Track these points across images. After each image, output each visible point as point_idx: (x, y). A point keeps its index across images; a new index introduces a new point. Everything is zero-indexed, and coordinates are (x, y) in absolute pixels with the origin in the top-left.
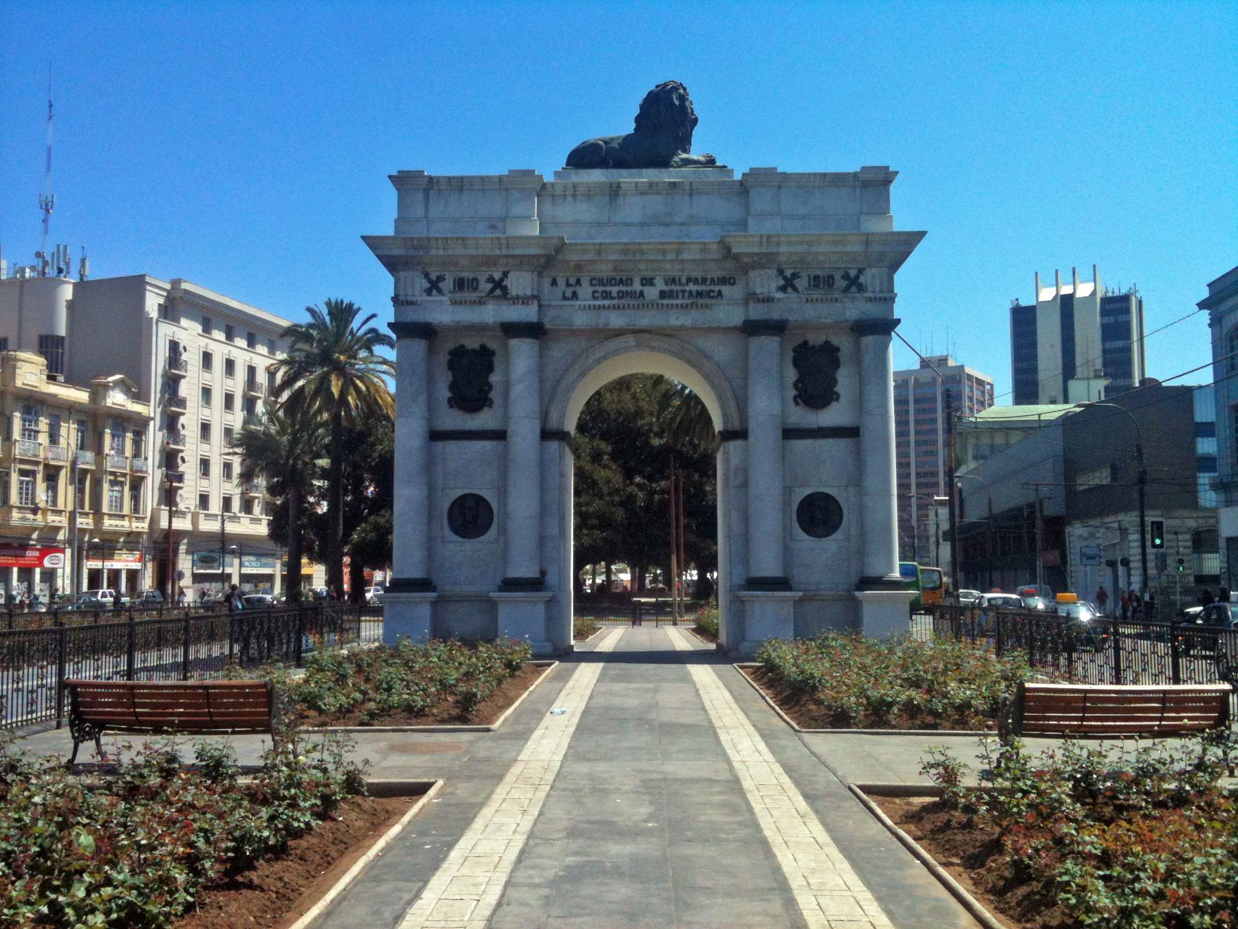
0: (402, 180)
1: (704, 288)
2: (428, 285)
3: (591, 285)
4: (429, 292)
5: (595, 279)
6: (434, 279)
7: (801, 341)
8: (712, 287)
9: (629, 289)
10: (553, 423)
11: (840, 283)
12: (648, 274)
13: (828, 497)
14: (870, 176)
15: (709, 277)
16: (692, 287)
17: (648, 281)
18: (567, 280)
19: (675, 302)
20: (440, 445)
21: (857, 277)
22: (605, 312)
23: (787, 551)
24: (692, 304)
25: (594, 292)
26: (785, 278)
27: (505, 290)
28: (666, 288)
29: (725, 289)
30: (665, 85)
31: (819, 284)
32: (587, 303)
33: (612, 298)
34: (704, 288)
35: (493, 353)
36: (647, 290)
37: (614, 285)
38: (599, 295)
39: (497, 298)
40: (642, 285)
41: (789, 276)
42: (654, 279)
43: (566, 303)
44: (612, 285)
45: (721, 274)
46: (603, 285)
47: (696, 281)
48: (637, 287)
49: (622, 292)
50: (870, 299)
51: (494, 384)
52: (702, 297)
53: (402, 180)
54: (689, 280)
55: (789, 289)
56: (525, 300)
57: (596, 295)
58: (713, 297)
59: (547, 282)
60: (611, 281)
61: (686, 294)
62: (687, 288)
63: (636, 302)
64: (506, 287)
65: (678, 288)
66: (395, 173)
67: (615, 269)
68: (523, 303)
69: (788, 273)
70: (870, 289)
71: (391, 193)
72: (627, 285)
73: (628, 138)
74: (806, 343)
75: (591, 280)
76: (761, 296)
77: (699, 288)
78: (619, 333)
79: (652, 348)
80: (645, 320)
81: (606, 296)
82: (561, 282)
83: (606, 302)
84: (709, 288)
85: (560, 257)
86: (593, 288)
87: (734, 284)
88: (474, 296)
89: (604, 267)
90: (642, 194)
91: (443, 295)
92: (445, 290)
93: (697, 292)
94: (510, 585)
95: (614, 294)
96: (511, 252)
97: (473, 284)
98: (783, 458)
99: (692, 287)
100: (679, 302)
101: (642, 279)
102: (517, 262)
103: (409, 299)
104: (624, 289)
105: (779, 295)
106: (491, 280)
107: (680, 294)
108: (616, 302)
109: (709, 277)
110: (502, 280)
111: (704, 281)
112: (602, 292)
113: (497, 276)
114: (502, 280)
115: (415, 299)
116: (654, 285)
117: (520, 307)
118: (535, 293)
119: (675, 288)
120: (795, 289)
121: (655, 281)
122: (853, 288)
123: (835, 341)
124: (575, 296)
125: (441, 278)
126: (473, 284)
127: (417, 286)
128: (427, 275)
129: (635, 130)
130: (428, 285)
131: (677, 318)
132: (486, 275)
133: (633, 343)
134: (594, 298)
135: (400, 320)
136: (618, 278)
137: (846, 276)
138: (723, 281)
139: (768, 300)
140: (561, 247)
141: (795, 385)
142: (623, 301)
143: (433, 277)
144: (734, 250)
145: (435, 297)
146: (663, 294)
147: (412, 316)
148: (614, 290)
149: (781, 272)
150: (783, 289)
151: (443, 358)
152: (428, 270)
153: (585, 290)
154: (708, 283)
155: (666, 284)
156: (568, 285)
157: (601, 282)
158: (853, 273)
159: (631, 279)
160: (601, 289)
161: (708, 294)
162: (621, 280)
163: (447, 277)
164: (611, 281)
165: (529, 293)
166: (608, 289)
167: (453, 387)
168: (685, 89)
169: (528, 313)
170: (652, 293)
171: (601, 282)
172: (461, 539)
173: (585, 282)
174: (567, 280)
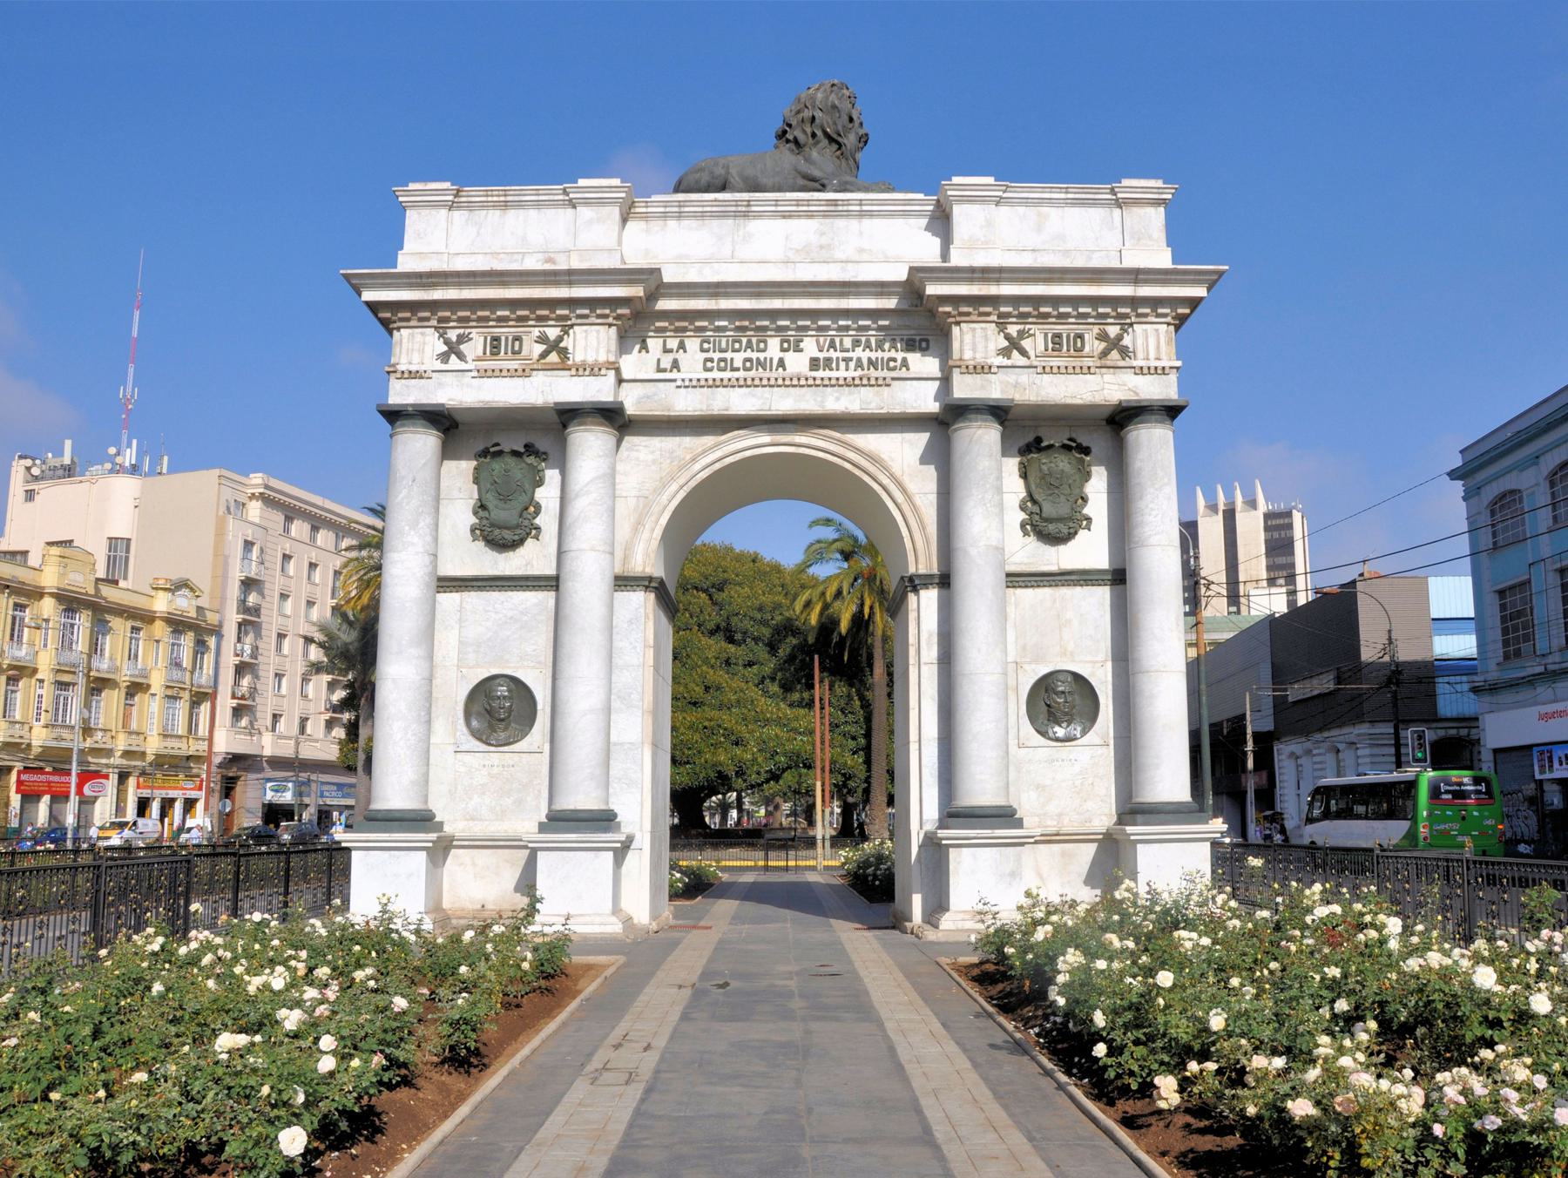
1: (879, 354)
2: (445, 348)
8: (893, 354)
9: (762, 356)
19: (834, 374)
27: (563, 353)
28: (821, 355)
33: (734, 369)
36: (790, 357)
37: (738, 351)
38: (715, 364)
40: (783, 350)
41: (1015, 335)
44: (734, 351)
46: (721, 351)
47: (868, 346)
51: (543, 503)
54: (856, 343)
55: (1015, 353)
56: (594, 370)
57: (709, 365)
58: (894, 369)
61: (852, 365)
64: (566, 349)
65: (841, 355)
68: (592, 374)
70: (1140, 354)
76: (972, 363)
77: (873, 355)
81: (725, 365)
83: (727, 375)
84: (887, 355)
93: (869, 359)
95: (736, 365)
100: (842, 373)
103: (413, 368)
104: (754, 355)
105: (1001, 361)
106: (542, 339)
107: (842, 365)
108: (741, 374)
110: (560, 339)
112: (721, 360)
114: (560, 339)
115: (422, 368)
116: (801, 351)
118: (612, 359)
119: (833, 354)
122: (1115, 354)
127: (428, 349)
130: (445, 348)
131: (838, 399)
132: (536, 332)
134: (707, 370)
139: (982, 369)
142: (753, 373)
143: (453, 335)
146: (814, 364)
148: (738, 359)
150: (1005, 352)
156: (666, 351)
159: (765, 342)
160: (717, 356)
161: (888, 364)
165: (602, 358)
166: (728, 355)
170: (797, 363)
173: (693, 344)
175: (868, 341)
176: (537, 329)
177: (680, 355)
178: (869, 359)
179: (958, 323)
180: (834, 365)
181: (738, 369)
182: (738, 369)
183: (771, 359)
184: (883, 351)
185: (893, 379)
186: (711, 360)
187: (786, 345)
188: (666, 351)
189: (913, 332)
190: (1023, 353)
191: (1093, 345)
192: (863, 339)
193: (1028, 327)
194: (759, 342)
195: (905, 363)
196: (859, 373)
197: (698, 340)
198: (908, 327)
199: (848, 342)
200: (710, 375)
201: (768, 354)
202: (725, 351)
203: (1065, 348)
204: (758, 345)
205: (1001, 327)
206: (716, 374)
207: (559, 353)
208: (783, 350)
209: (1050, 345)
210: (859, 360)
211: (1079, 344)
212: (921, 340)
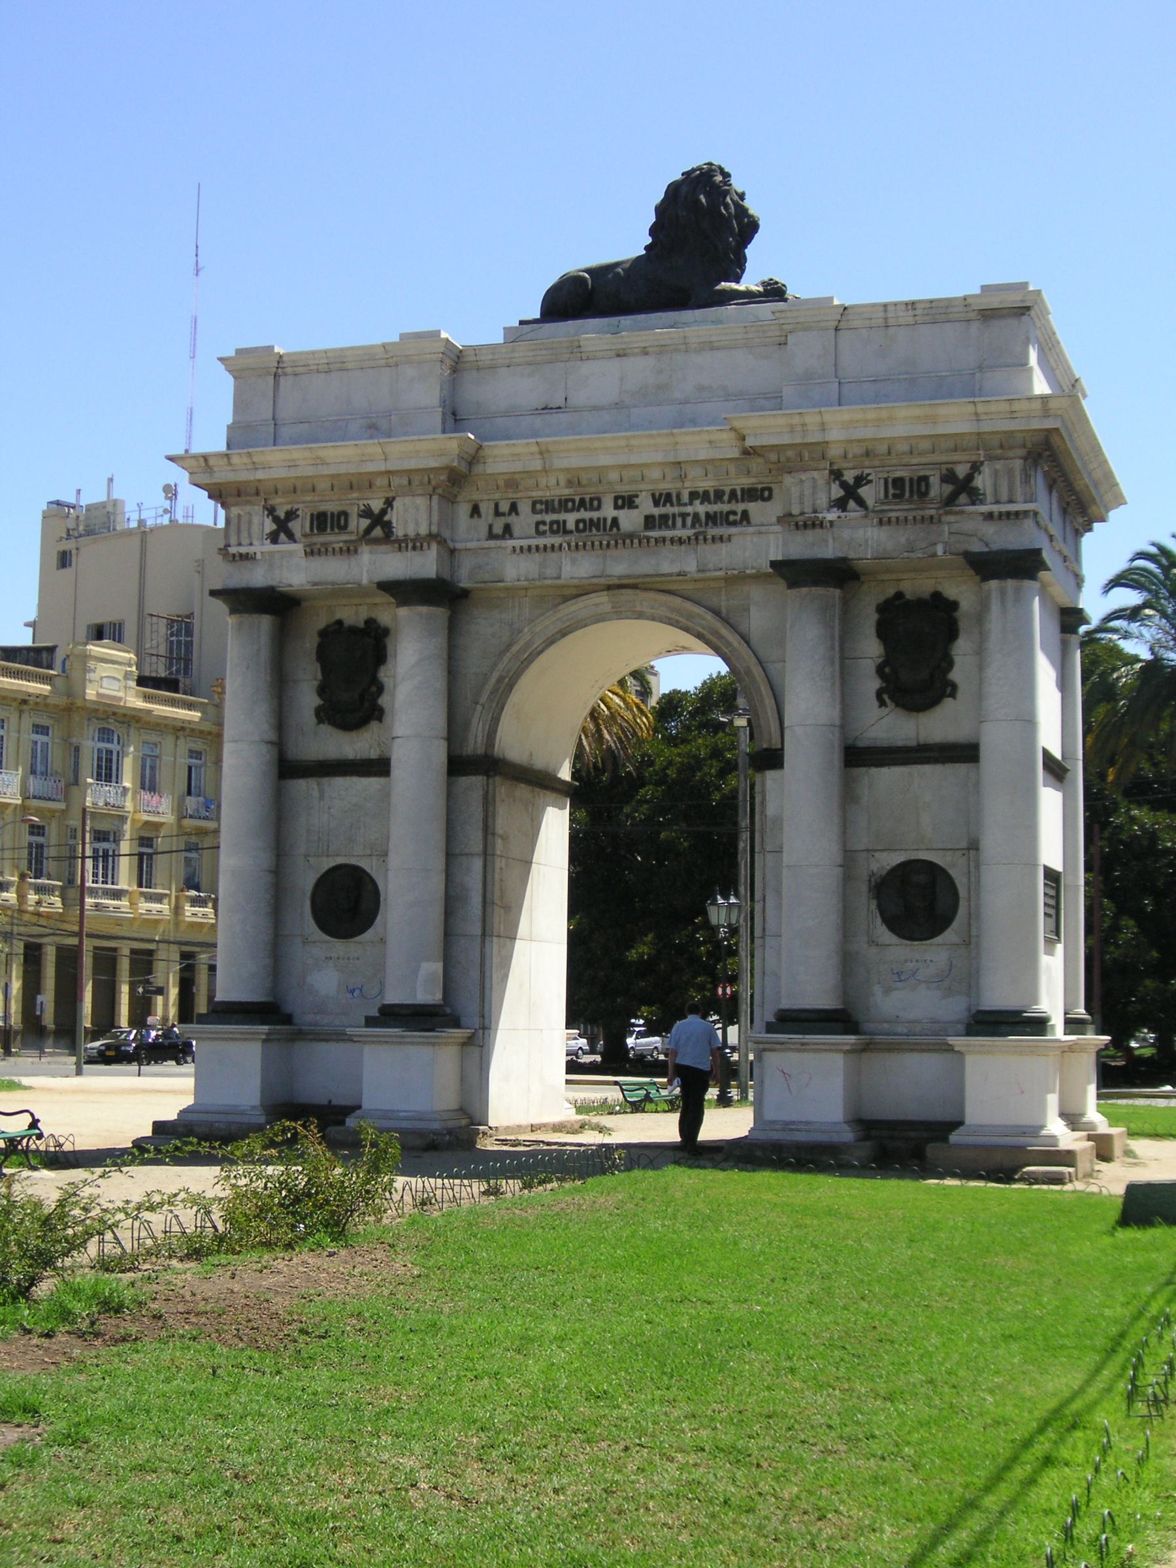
3: (534, 511)
5: (541, 502)
6: (282, 516)
7: (890, 592)
8: (733, 506)
9: (595, 515)
10: (474, 744)
11: (937, 489)
12: (625, 489)
13: (931, 868)
14: (995, 302)
15: (727, 489)
16: (701, 508)
17: (627, 502)
18: (497, 506)
19: (668, 534)
20: (302, 787)
21: (970, 478)
22: (554, 556)
23: (848, 962)
24: (696, 535)
25: (538, 524)
26: (844, 485)
27: (388, 527)
28: (656, 511)
29: (753, 507)
30: (693, 170)
32: (525, 543)
33: (566, 532)
35: (386, 632)
37: (572, 510)
38: (547, 528)
39: (376, 541)
40: (616, 507)
41: (851, 482)
42: (637, 496)
43: (492, 543)
44: (567, 511)
45: (746, 482)
46: (554, 511)
47: (705, 497)
49: (583, 521)
50: (989, 516)
52: (715, 524)
55: (852, 504)
56: (416, 543)
57: (542, 528)
58: (734, 523)
59: (464, 510)
60: (565, 505)
62: (689, 509)
64: (389, 523)
65: (676, 510)
66: (231, 353)
67: (570, 483)
68: (414, 548)
69: (849, 476)
70: (989, 498)
71: (227, 383)
72: (592, 509)
73: (639, 258)
74: (899, 595)
75: (534, 504)
76: (801, 518)
78: (582, 591)
79: (640, 616)
80: (620, 565)
82: (486, 509)
85: (478, 469)
86: (539, 517)
87: (769, 498)
88: (336, 539)
90: (618, 356)
91: (295, 541)
93: (707, 514)
95: (571, 525)
96: (391, 466)
97: (339, 521)
98: (848, 797)
99: (701, 508)
100: (679, 533)
101: (616, 499)
102: (405, 481)
106: (367, 513)
107: (679, 521)
109: (727, 489)
110: (384, 512)
112: (552, 523)
113: (377, 505)
114: (384, 512)
115: (251, 550)
116: (637, 507)
117: (410, 554)
118: (434, 529)
119: (669, 510)
120: (861, 503)
121: (637, 501)
122: (963, 498)
123: (951, 591)
124: (508, 531)
125: (291, 515)
127: (255, 528)
128: (271, 511)
129: (646, 248)
133: (608, 608)
134: (539, 533)
136: (577, 499)
137: (949, 477)
138: (752, 494)
141: (880, 670)
143: (281, 514)
144: (749, 442)
145: (285, 547)
146: (649, 522)
148: (571, 519)
149: (836, 475)
150: (841, 504)
151: (311, 643)
152: (271, 502)
153: (524, 521)
154: (726, 498)
155: (656, 503)
156: (497, 513)
158: (962, 471)
159: (599, 500)
161: (723, 519)
162: (582, 501)
163: (299, 512)
165: (423, 531)
166: (562, 516)
167: (322, 691)
168: (726, 175)
171: (549, 506)
172: (328, 938)
174: (497, 506)
176: (361, 503)
177: (512, 519)
178: (707, 514)
180: (670, 522)
182: (571, 532)
183: (605, 519)
184: (723, 503)
186: (544, 523)
189: (753, 480)
196: (698, 529)
200: (541, 541)
202: (559, 512)
203: (907, 494)
207: (383, 528)
208: (616, 507)
209: (891, 491)
211: (923, 489)
212: (763, 490)
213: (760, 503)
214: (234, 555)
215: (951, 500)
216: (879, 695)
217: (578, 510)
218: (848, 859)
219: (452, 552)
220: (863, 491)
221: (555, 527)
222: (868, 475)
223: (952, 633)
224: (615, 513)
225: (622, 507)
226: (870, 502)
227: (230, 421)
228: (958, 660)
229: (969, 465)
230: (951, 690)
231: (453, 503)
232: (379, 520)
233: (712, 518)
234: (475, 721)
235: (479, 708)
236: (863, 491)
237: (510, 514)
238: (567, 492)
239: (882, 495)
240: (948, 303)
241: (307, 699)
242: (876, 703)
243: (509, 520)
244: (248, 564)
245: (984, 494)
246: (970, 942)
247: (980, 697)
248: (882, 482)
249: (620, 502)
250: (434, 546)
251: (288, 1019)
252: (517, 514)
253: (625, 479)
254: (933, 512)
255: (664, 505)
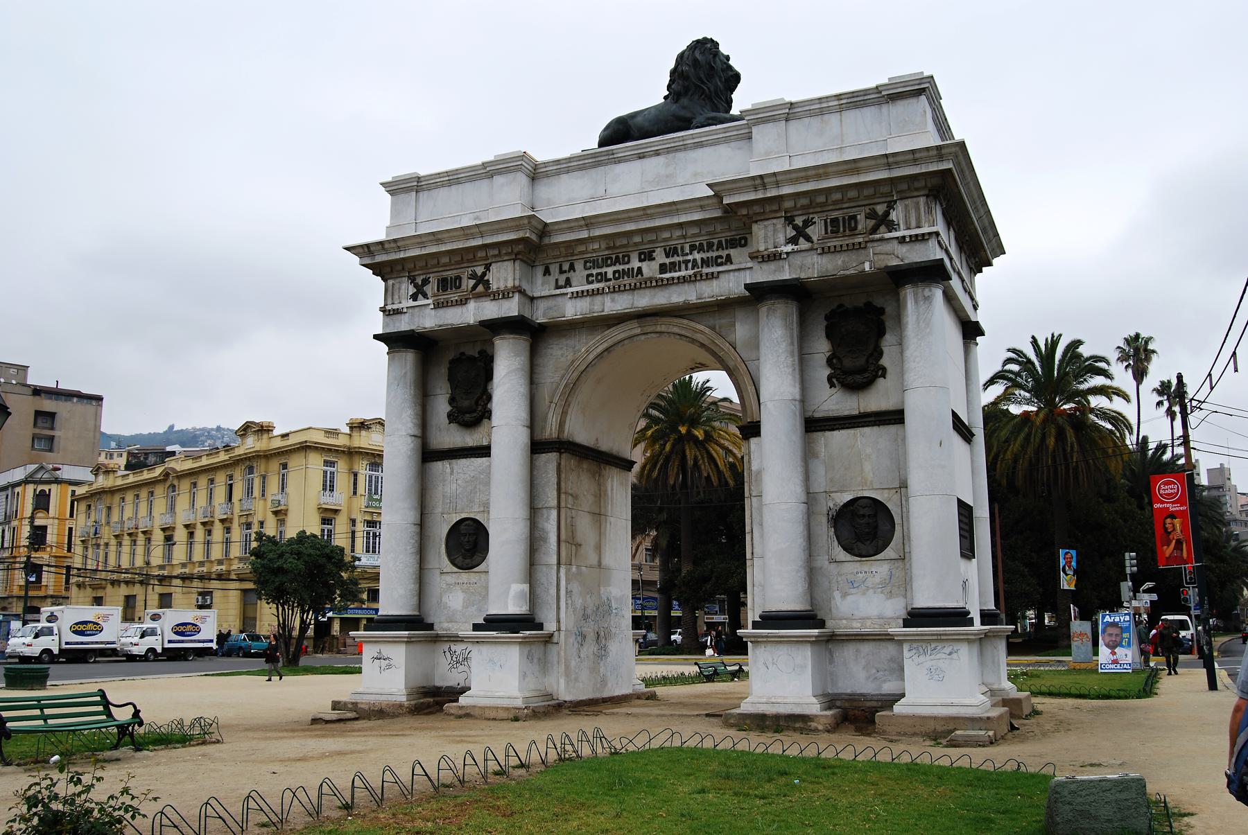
0: (396, 188)
1: (709, 254)
4: (414, 297)
8: (720, 253)
9: (626, 267)
16: (698, 256)
17: (647, 256)
18: (561, 267)
19: (676, 275)
20: (440, 467)
22: (599, 298)
23: (812, 574)
24: (695, 275)
25: (588, 276)
26: (795, 227)
27: (487, 284)
28: (667, 261)
29: (732, 252)
31: (838, 232)
32: (579, 289)
34: (709, 254)
38: (594, 278)
39: (478, 296)
41: (801, 224)
42: (654, 251)
43: (558, 292)
44: (608, 266)
46: (599, 267)
47: (701, 249)
48: (635, 264)
49: (618, 271)
50: (902, 240)
53: (396, 188)
54: (693, 248)
55: (801, 240)
56: (505, 294)
57: (591, 279)
58: (721, 264)
61: (690, 265)
62: (690, 257)
63: (633, 281)
64: (488, 281)
65: (681, 259)
66: (390, 179)
75: (586, 263)
76: (766, 253)
77: (704, 256)
80: (645, 300)
81: (602, 278)
84: (715, 254)
85: (546, 241)
89: (596, 246)
90: (640, 158)
92: (430, 294)
93: (702, 258)
94: (494, 623)
95: (610, 275)
98: (808, 455)
100: (683, 273)
104: (620, 267)
105: (789, 248)
106: (473, 276)
107: (683, 266)
110: (484, 274)
111: (710, 246)
112: (598, 274)
113: (480, 270)
114: (484, 274)
115: (400, 306)
116: (654, 259)
118: (517, 283)
119: (676, 259)
122: (883, 228)
124: (568, 283)
125: (426, 282)
126: (456, 282)
134: (589, 283)
135: (392, 329)
139: (775, 257)
140: (545, 230)
141: (830, 362)
143: (419, 281)
146: (663, 268)
147: (403, 324)
148: (610, 271)
150: (793, 241)
154: (715, 248)
155: (667, 256)
156: (562, 272)
157: (596, 264)
160: (594, 272)
161: (715, 262)
164: (606, 262)
165: (510, 284)
167: (452, 401)
169: (511, 308)
170: (650, 269)
173: (579, 266)
175: (701, 245)
176: (470, 269)
177: (571, 275)
178: (702, 259)
179: (756, 222)
180: (677, 268)
181: (610, 280)
182: (610, 280)
183: (633, 269)
184: (713, 251)
185: (718, 272)
186: (592, 275)
187: (643, 257)
188: (562, 272)
189: (733, 233)
190: (808, 239)
191: (863, 223)
192: (697, 244)
193: (811, 216)
194: (624, 256)
195: (729, 259)
197: (582, 262)
198: (729, 229)
199: (687, 250)
201: (629, 266)
203: (841, 229)
204: (623, 260)
205: (789, 220)
206: (595, 286)
208: (641, 260)
209: (829, 229)
210: (695, 260)
211: (853, 225)
212: (741, 239)
213: (739, 249)
214: (389, 310)
215: (874, 230)
216: (830, 379)
217: (615, 265)
218: (810, 499)
219: (532, 299)
220: (809, 231)
221: (599, 277)
222: (813, 218)
223: (881, 333)
224: (639, 264)
225: (644, 260)
226: (815, 238)
227: (388, 224)
228: (886, 350)
229: (886, 205)
230: (883, 372)
231: (532, 267)
232: (481, 280)
233: (705, 262)
234: (550, 415)
235: (553, 405)
236: (809, 231)
237: (569, 272)
238: (606, 253)
239: (823, 232)
240: (866, 92)
241: (441, 407)
242: (828, 386)
243: (568, 275)
244: (398, 317)
245: (898, 225)
246: (903, 558)
247: (902, 374)
248: (823, 222)
249: (643, 257)
250: (517, 296)
251: (430, 627)
252: (574, 271)
253: (645, 241)
254: (861, 240)
255: (673, 256)
